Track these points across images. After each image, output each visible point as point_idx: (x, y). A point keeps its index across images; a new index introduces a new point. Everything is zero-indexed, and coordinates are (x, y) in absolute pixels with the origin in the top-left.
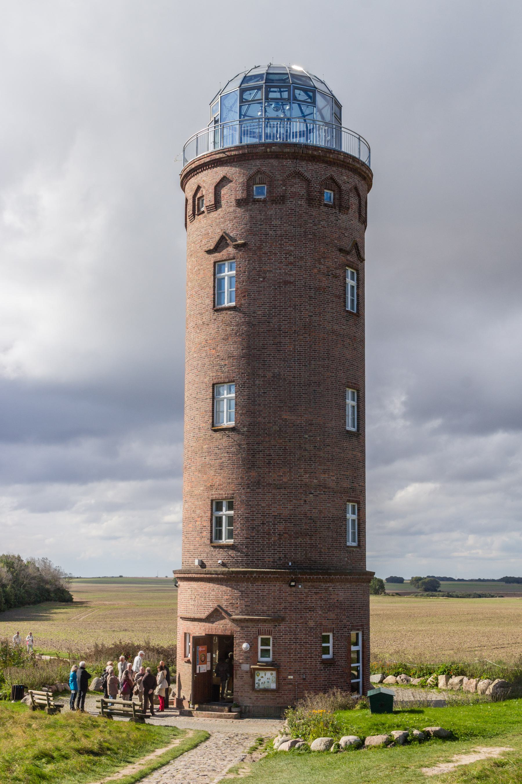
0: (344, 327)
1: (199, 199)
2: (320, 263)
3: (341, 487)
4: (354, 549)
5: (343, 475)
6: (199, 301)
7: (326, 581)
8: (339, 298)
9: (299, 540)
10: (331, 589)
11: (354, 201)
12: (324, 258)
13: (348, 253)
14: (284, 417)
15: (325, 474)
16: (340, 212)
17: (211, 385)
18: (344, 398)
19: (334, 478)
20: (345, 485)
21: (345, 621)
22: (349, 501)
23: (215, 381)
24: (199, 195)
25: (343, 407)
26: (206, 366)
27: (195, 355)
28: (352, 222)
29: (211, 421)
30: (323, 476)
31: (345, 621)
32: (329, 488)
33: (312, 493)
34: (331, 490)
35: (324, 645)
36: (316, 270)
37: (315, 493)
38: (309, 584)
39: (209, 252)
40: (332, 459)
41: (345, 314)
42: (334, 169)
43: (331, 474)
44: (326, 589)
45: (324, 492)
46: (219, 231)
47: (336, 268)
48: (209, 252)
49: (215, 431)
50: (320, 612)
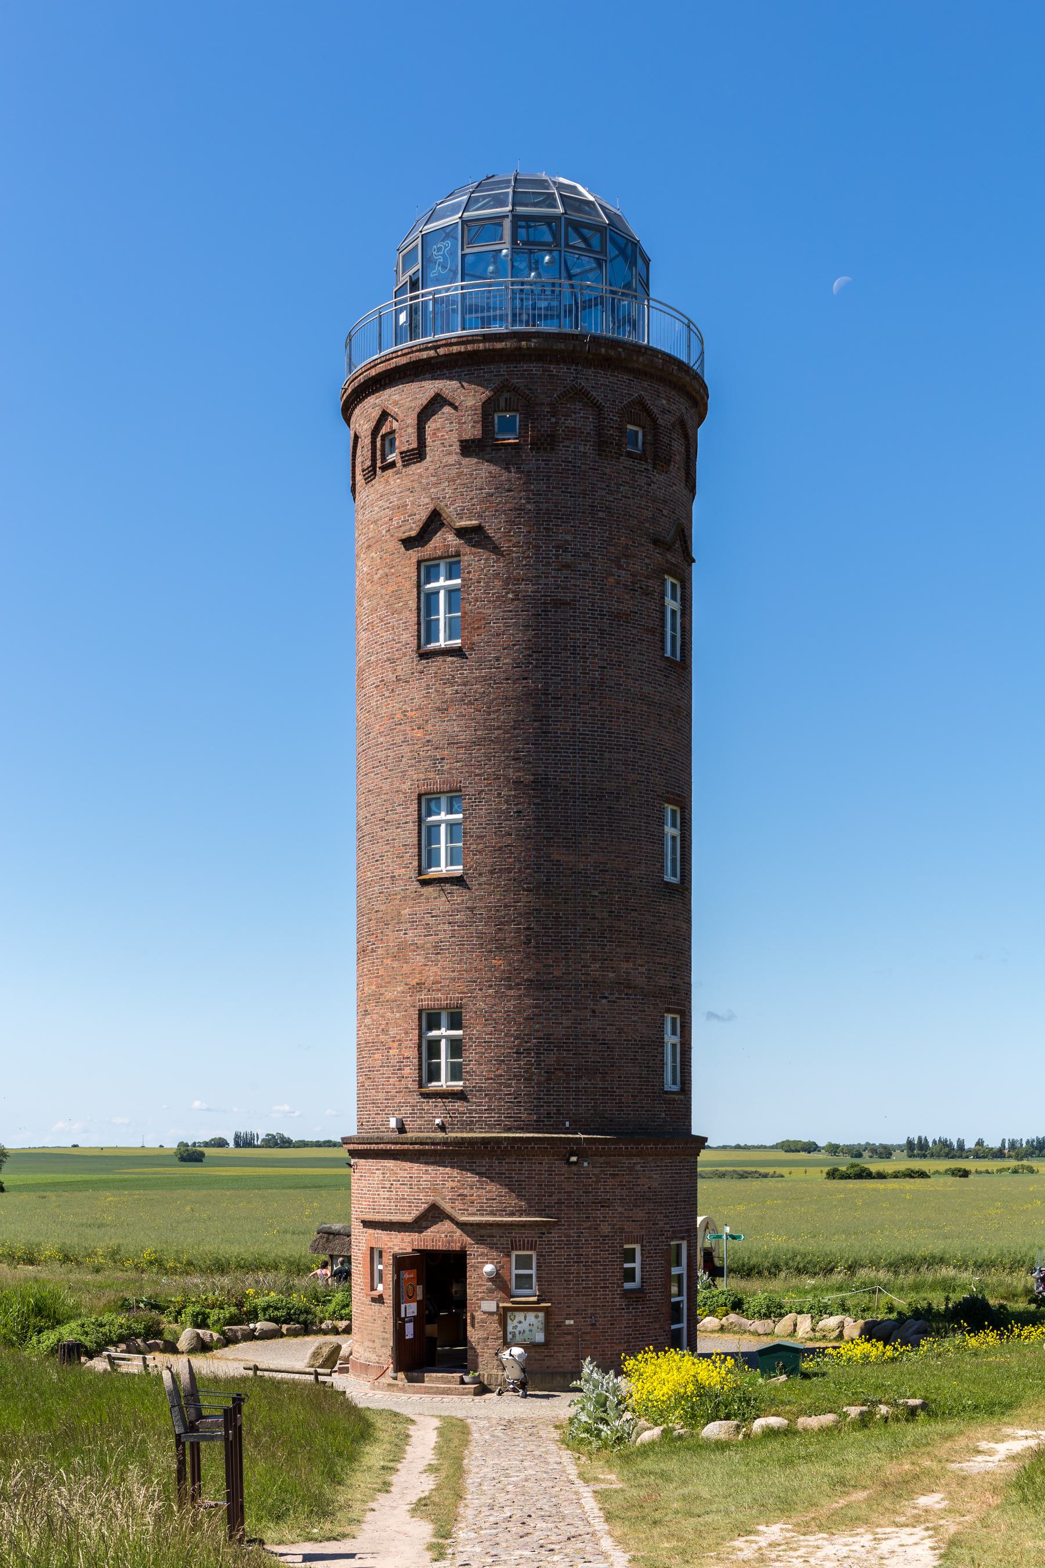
1: (383, 437)
2: (620, 567)
6: (386, 636)
8: (653, 634)
9: (582, 1083)
10: (638, 1167)
11: (678, 446)
12: (627, 556)
13: (669, 548)
14: (555, 857)
15: (627, 961)
16: (654, 468)
17: (414, 796)
18: (662, 823)
19: (643, 969)
21: (661, 1224)
22: (669, 1011)
23: (423, 789)
24: (383, 431)
25: (661, 838)
26: (404, 760)
27: (381, 740)
29: (416, 863)
30: (624, 965)
31: (661, 1224)
32: (635, 988)
33: (606, 998)
35: (626, 1265)
36: (611, 580)
37: (612, 998)
38: (602, 1159)
39: (409, 543)
43: (639, 961)
46: (427, 500)
48: (409, 543)
49: (425, 883)
50: (620, 1210)
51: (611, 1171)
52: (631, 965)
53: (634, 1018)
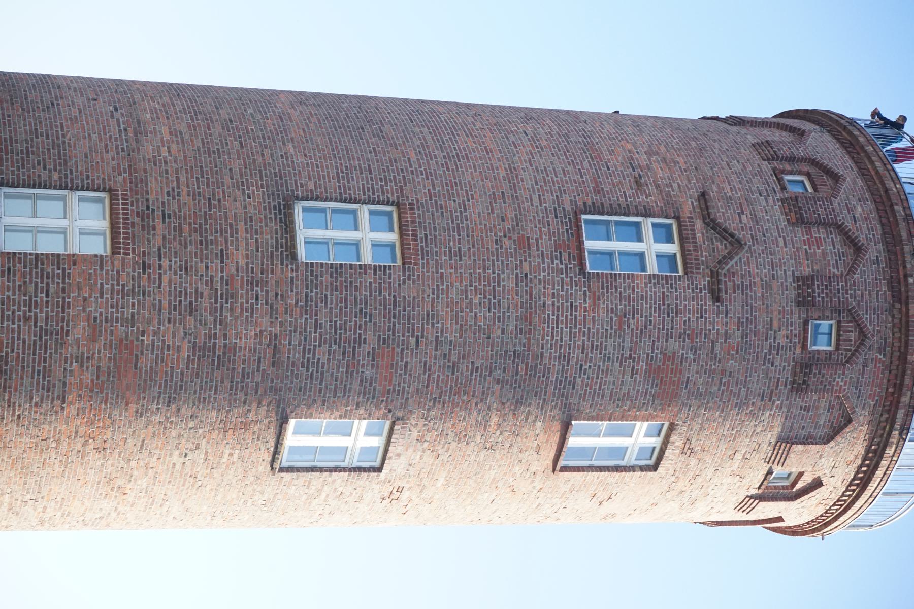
2: (649, 153)
3: (145, 171)
5: (177, 178)
15: (171, 133)
16: (783, 201)
19: (165, 153)
20: (153, 185)
28: (781, 240)
30: (165, 130)
34: (134, 144)
41: (568, 207)
42: (860, 183)
43: (174, 147)
45: (125, 130)
47: (658, 187)
52: (167, 137)
53: (95, 137)
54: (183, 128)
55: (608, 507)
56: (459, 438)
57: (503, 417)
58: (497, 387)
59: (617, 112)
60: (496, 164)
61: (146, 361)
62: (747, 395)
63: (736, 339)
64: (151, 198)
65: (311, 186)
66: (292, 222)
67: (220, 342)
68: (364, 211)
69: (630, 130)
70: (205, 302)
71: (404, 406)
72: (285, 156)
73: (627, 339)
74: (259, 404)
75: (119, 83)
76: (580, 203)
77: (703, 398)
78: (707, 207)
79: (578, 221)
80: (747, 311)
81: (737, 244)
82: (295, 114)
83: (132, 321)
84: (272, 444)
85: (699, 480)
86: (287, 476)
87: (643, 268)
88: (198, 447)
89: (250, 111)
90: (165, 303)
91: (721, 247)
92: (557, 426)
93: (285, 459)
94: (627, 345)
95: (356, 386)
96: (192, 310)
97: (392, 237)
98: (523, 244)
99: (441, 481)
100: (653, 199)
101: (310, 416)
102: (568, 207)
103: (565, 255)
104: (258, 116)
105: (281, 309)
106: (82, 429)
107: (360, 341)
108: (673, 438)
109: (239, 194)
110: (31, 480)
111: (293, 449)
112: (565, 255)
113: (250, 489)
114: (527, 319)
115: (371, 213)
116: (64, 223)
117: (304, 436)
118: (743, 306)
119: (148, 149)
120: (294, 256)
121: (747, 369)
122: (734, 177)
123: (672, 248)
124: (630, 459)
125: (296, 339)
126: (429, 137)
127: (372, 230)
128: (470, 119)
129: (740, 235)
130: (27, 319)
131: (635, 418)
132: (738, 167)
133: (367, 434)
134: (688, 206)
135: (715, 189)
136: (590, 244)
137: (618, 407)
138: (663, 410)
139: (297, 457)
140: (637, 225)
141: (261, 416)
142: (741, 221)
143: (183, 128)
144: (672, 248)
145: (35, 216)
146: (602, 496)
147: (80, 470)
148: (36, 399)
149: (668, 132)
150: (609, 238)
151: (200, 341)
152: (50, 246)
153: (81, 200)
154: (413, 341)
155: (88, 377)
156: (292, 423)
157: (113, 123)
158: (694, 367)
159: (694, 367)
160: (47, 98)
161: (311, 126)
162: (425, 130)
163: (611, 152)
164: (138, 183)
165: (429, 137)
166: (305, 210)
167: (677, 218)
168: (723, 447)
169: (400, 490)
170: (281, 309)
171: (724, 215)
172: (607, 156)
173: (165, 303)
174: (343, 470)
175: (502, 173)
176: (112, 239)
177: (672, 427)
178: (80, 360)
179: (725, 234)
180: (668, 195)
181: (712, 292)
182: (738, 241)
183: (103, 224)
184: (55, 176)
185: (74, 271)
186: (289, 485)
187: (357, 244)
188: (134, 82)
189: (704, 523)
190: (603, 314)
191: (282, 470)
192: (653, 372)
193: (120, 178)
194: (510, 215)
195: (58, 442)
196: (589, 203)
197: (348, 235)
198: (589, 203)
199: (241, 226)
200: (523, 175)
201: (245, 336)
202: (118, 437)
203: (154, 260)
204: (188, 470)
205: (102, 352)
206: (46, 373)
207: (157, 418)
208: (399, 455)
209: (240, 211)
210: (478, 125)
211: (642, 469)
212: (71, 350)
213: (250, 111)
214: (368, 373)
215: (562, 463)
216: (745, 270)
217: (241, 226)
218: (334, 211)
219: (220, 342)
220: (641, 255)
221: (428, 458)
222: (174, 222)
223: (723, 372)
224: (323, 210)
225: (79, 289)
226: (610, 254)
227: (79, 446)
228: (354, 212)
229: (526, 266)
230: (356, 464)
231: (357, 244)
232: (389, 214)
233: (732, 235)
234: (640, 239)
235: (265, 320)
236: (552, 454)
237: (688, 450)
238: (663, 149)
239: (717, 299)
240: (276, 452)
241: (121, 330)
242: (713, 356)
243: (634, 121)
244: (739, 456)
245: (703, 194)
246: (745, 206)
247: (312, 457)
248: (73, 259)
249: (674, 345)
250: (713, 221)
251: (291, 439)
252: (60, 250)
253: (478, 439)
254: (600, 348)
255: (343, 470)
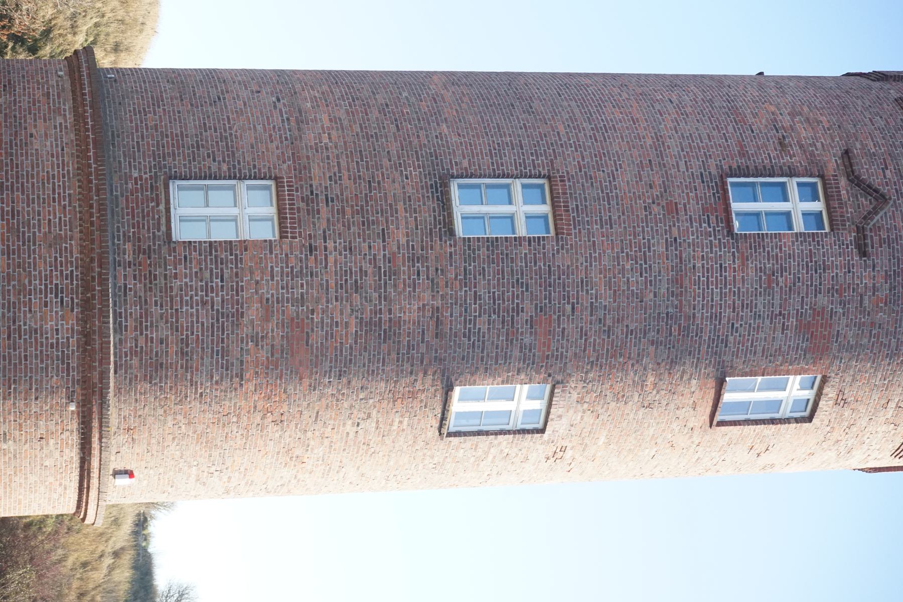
0: (683, 168)
2: (792, 115)
3: (308, 157)
4: (162, 207)
5: (338, 163)
7: (75, 108)
10: (59, 120)
15: (331, 120)
20: (316, 171)
30: (325, 118)
34: (297, 133)
38: (68, 85)
40: (368, 137)
41: (714, 171)
43: (334, 133)
44: (58, 111)
45: (288, 119)
47: (801, 146)
51: (53, 92)
52: (327, 124)
53: (259, 128)
54: (342, 114)
55: (765, 459)
56: (617, 398)
57: (659, 376)
58: (652, 349)
59: (761, 74)
60: (643, 133)
61: (317, 337)
62: (897, 346)
63: (884, 292)
64: (315, 183)
65: (465, 163)
66: (449, 200)
67: (385, 317)
68: (517, 185)
69: (773, 92)
70: (370, 280)
71: (563, 370)
72: (439, 136)
73: (777, 297)
74: (425, 373)
75: (280, 73)
76: (726, 167)
77: (853, 350)
78: (851, 165)
79: (724, 184)
80: (894, 264)
81: (881, 199)
82: (448, 95)
83: (302, 300)
84: (439, 411)
85: (854, 429)
86: (455, 440)
87: (790, 228)
88: (369, 416)
89: (405, 94)
90: (332, 283)
91: (866, 203)
92: (711, 383)
93: (452, 424)
94: (777, 302)
95: (516, 353)
96: (357, 288)
97: (546, 209)
98: (672, 209)
99: (602, 440)
100: (798, 160)
101: (474, 384)
102: (714, 171)
103: (713, 218)
104: (413, 100)
105: (442, 284)
106: (260, 404)
107: (518, 310)
108: (826, 390)
109: (397, 175)
110: (215, 453)
111: (459, 415)
112: (713, 218)
113: (420, 454)
114: (678, 281)
115: (524, 186)
116: (235, 211)
117: (470, 402)
118: (890, 260)
119: (310, 137)
120: (452, 232)
121: (897, 320)
122: (877, 133)
123: (818, 206)
124: (785, 411)
125: (457, 310)
126: (576, 111)
127: (525, 203)
128: (616, 90)
129: (884, 190)
130: (204, 303)
131: (788, 373)
132: (882, 123)
133: (530, 397)
134: (832, 164)
135: (858, 146)
136: (737, 206)
137: (771, 362)
138: (814, 363)
139: (464, 422)
140: (783, 185)
141: (428, 385)
142: (885, 176)
143: (342, 114)
144: (818, 206)
145: (207, 206)
146: (759, 448)
147: (260, 442)
148: (216, 378)
149: (812, 92)
150: (755, 200)
151: (367, 316)
152: (223, 233)
153: (249, 188)
154: (568, 308)
155: (263, 355)
156: (457, 390)
157: (276, 114)
158: (844, 321)
159: (844, 321)
160: (214, 93)
161: (464, 106)
162: (573, 104)
163: (755, 115)
164: (302, 170)
165: (576, 111)
166: (460, 186)
167: (822, 176)
168: (875, 396)
169: (563, 449)
170: (442, 284)
171: (868, 171)
172: (751, 120)
173: (332, 283)
174: (509, 432)
175: (649, 142)
176: (280, 224)
177: (825, 380)
178: (255, 339)
179: (869, 190)
180: (812, 154)
181: (858, 247)
182: (883, 196)
183: (272, 211)
184: (225, 167)
185: (246, 256)
186: (457, 449)
187: (511, 218)
188: (295, 72)
189: (862, 470)
190: (752, 273)
191: (450, 435)
192: (805, 328)
193: (285, 166)
194: (658, 181)
195: (239, 416)
196: (735, 166)
197: (501, 210)
198: (735, 166)
199: (400, 206)
200: (669, 142)
201: (409, 310)
202: (294, 410)
203: (319, 242)
204: (361, 437)
205: (275, 331)
206: (225, 352)
207: (329, 391)
208: (560, 417)
209: (399, 192)
210: (625, 95)
211: (797, 420)
212: (246, 331)
213: (405, 94)
214: (527, 340)
215: (718, 418)
216: (891, 224)
217: (400, 206)
218: (488, 186)
219: (385, 317)
220: (788, 214)
221: (589, 418)
222: (337, 205)
223: (873, 324)
224: (478, 186)
225: (252, 273)
226: (757, 215)
227: (258, 419)
228: (507, 186)
229: (675, 231)
230: (519, 427)
231: (511, 218)
232: (541, 187)
233: (876, 191)
234: (786, 199)
235: (427, 295)
236: (709, 410)
237: (841, 401)
238: (806, 109)
239: (863, 254)
240: (443, 418)
241: (291, 309)
242: (863, 311)
243: (777, 83)
244: (892, 405)
245: (847, 152)
246: (888, 161)
247: (477, 422)
248: (244, 245)
249: (822, 300)
250: (858, 177)
251: (457, 406)
252: (233, 238)
253: (636, 398)
254: (750, 306)
255: (509, 432)
